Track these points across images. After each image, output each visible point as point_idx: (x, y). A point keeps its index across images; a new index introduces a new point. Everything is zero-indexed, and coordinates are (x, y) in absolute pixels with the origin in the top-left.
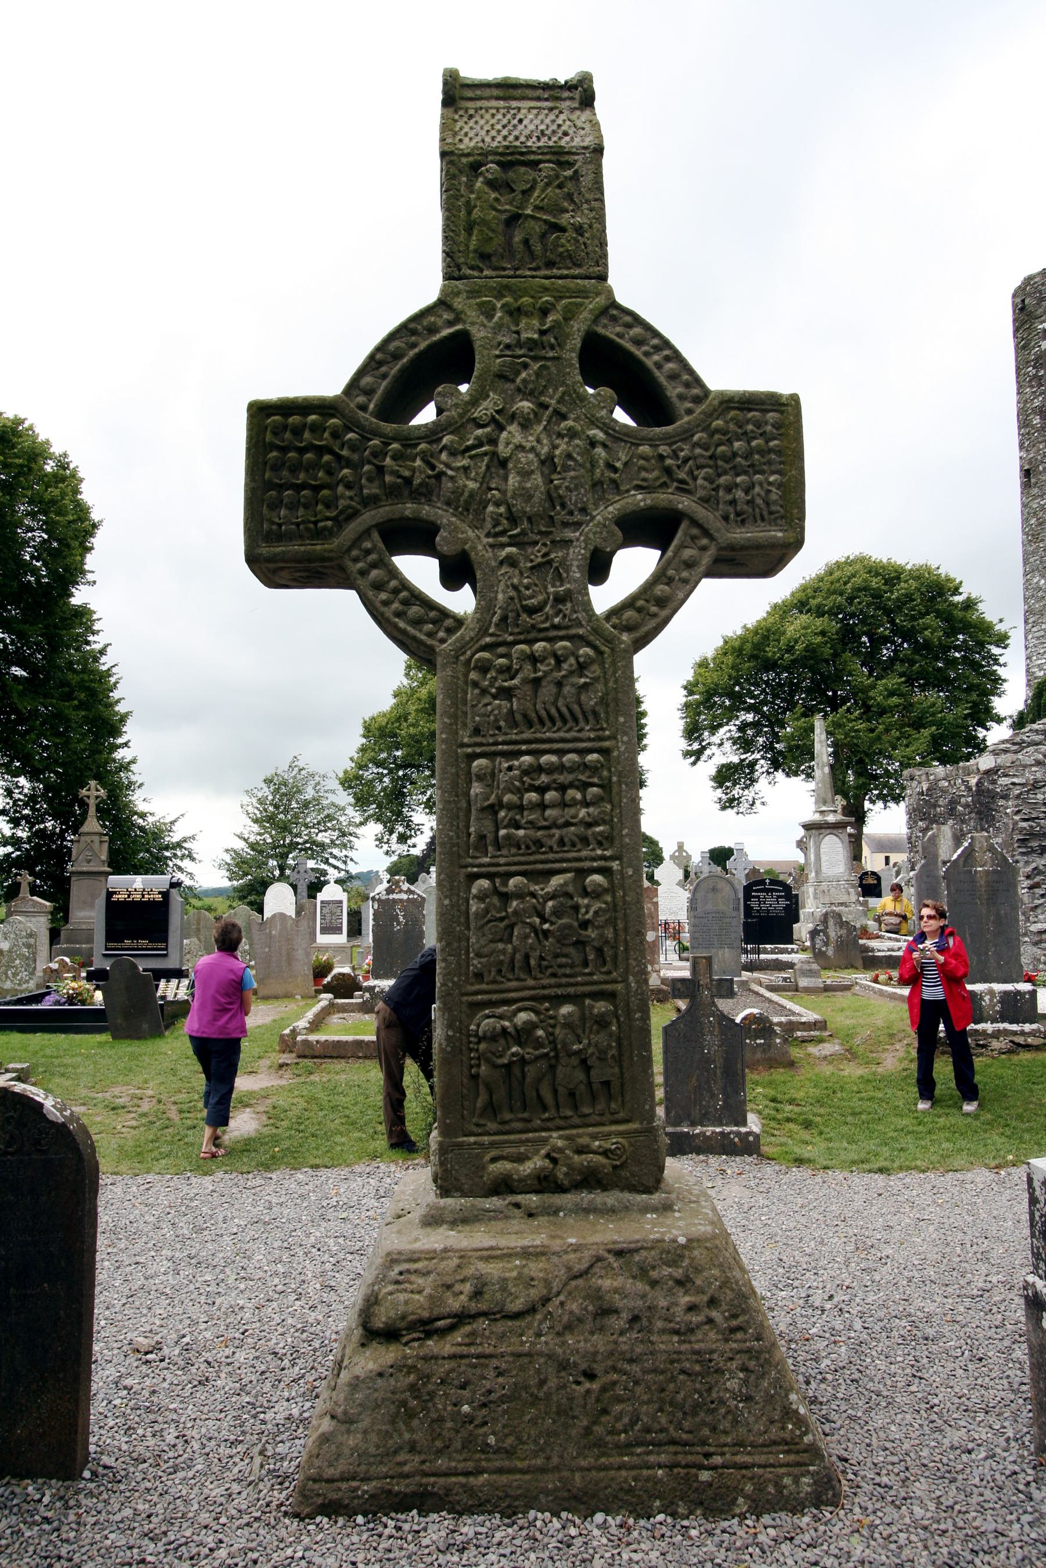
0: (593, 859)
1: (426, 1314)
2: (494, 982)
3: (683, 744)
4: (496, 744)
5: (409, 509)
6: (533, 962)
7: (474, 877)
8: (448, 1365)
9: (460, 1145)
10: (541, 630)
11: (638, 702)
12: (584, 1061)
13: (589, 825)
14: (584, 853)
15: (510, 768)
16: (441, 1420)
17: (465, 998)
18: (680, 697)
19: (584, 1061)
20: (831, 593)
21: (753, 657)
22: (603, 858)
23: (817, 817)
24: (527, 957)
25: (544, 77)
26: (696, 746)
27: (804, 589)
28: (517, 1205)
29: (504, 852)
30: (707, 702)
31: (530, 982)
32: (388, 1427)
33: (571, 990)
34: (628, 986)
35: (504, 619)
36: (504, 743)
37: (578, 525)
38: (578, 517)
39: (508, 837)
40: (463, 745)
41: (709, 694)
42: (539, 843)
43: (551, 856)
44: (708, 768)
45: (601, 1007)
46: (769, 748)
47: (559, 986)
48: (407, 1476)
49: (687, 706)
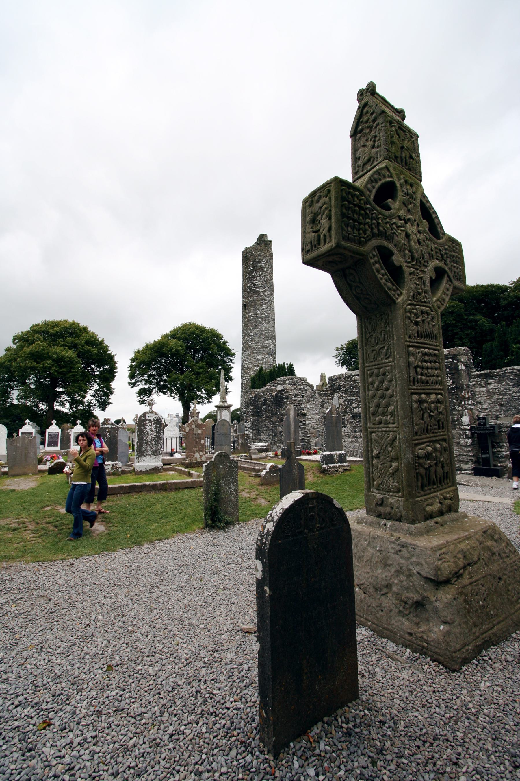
0: (438, 389)
1: (456, 570)
2: (420, 435)
3: (128, 380)
4: (415, 342)
5: (386, 243)
6: (429, 427)
7: (412, 393)
8: (470, 588)
9: (417, 502)
10: (422, 302)
11: (115, 363)
12: (442, 465)
13: (437, 376)
14: (437, 387)
15: (419, 352)
16: (477, 610)
17: (414, 442)
18: (129, 363)
19: (442, 465)
20: (182, 333)
21: (156, 352)
22: (440, 389)
23: (221, 404)
24: (428, 425)
25: (392, 104)
26: (133, 381)
27: (175, 330)
28: (436, 523)
29: (419, 384)
30: (139, 366)
31: (428, 435)
32: (465, 620)
33: (437, 438)
34: (449, 436)
35: (414, 295)
36: (417, 343)
37: (426, 266)
38: (426, 264)
39: (421, 379)
40: (406, 341)
41: (141, 363)
42: (427, 382)
43: (429, 387)
44: (136, 389)
45: (445, 444)
46: (157, 384)
47: (434, 436)
48: (478, 637)
49: (131, 366)
